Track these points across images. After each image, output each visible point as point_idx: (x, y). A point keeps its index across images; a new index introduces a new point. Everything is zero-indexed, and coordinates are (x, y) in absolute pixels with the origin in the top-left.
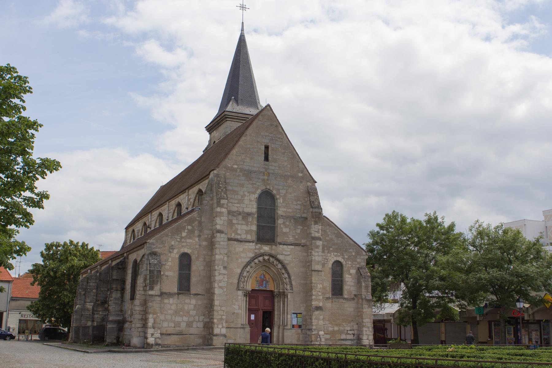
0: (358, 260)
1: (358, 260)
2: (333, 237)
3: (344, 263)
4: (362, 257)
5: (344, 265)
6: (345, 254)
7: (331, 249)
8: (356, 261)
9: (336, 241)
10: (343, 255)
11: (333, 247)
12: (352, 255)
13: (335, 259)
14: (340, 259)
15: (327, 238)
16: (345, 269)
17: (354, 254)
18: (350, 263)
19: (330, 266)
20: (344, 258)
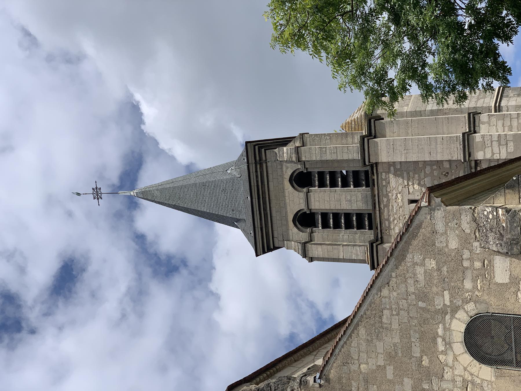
0: (454, 244)
1: (454, 244)
2: (380, 346)
3: (472, 309)
4: (440, 227)
5: (482, 309)
6: (439, 303)
7: (425, 362)
8: (459, 252)
9: (397, 340)
10: (443, 312)
11: (416, 352)
12: (439, 269)
13: (459, 348)
14: (458, 326)
15: (390, 375)
16: (494, 306)
17: (431, 264)
18: (468, 285)
19: (486, 372)
20: (455, 310)
